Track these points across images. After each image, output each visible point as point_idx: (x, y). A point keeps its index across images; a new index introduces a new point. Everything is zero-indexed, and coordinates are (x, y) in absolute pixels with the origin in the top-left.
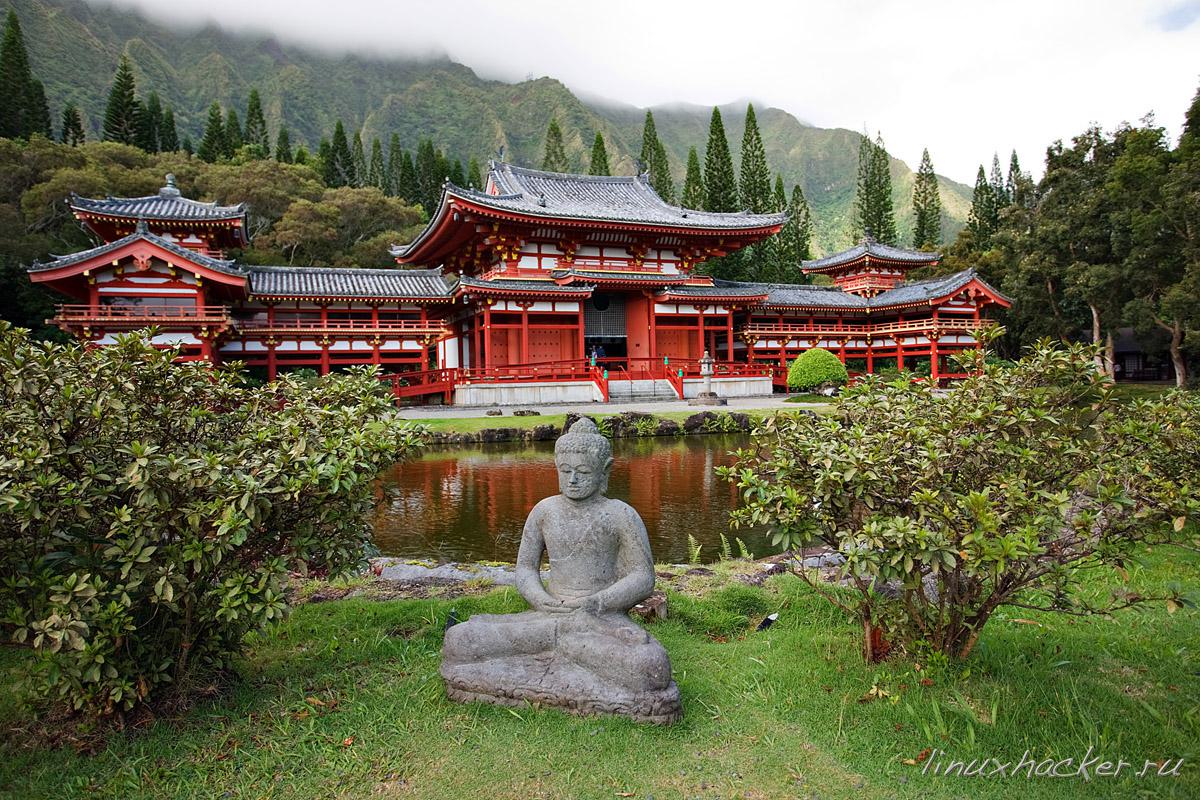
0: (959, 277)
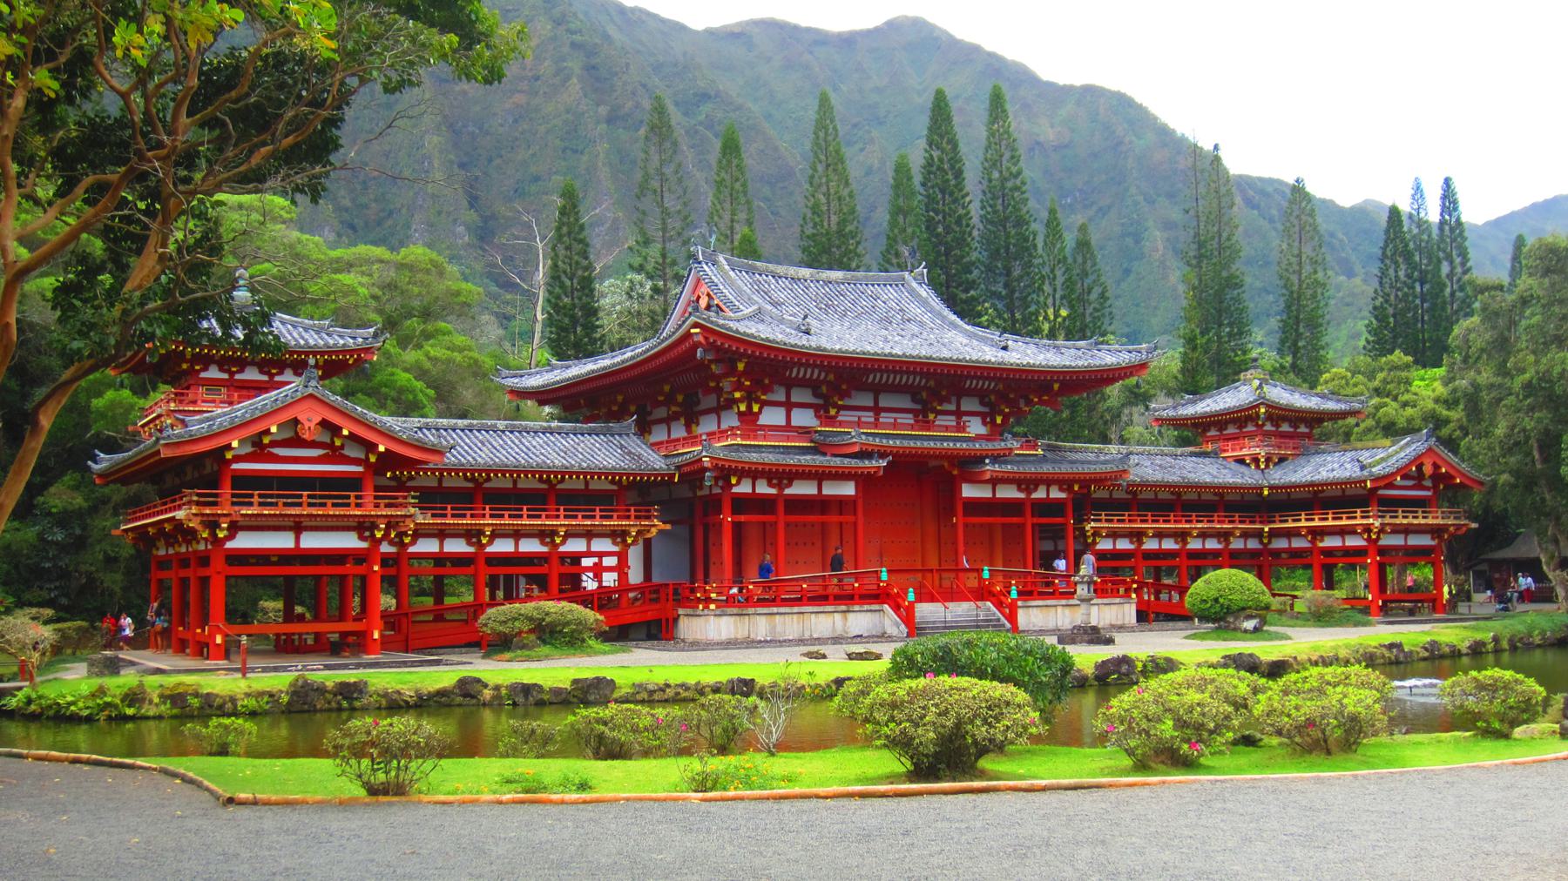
0: (1407, 444)
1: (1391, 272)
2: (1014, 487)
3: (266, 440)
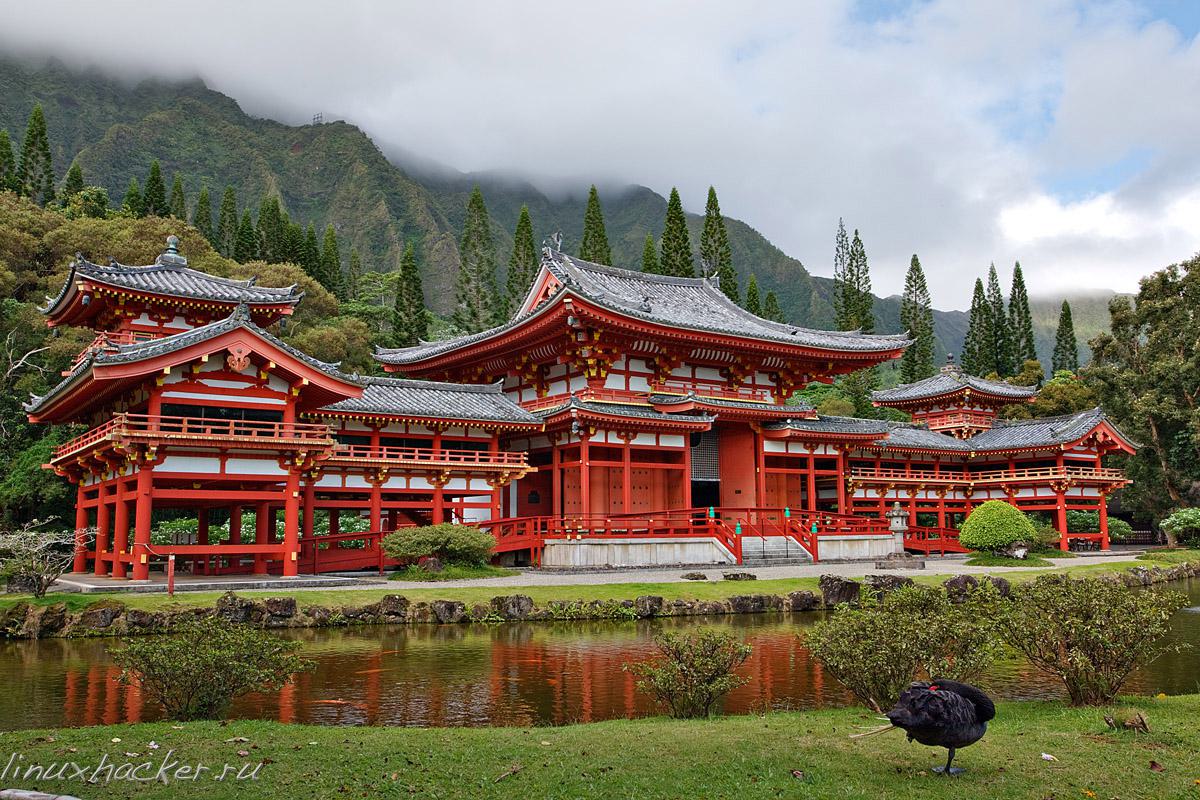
3: (196, 371)
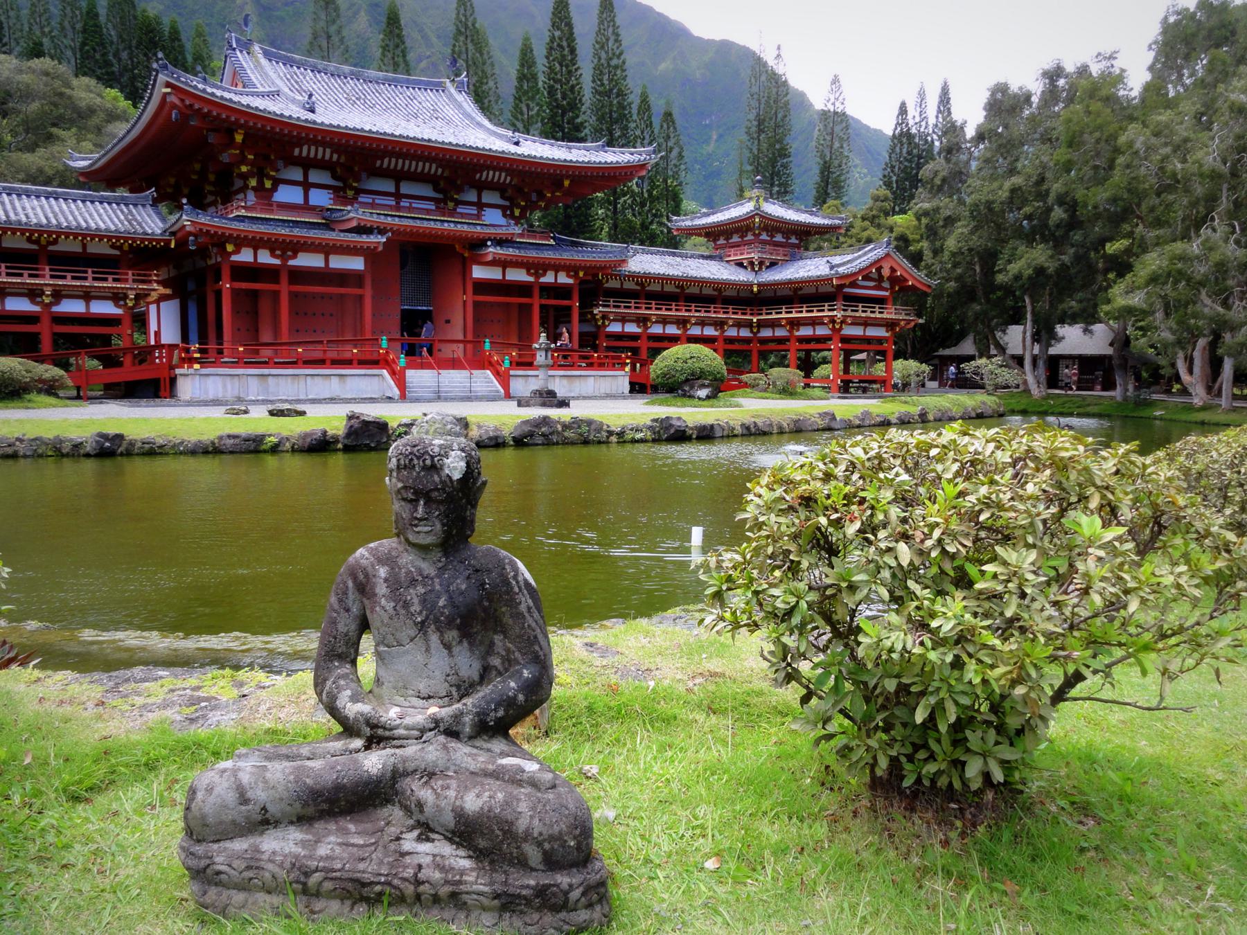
0: (870, 251)
1: (898, 149)
2: (524, 271)
